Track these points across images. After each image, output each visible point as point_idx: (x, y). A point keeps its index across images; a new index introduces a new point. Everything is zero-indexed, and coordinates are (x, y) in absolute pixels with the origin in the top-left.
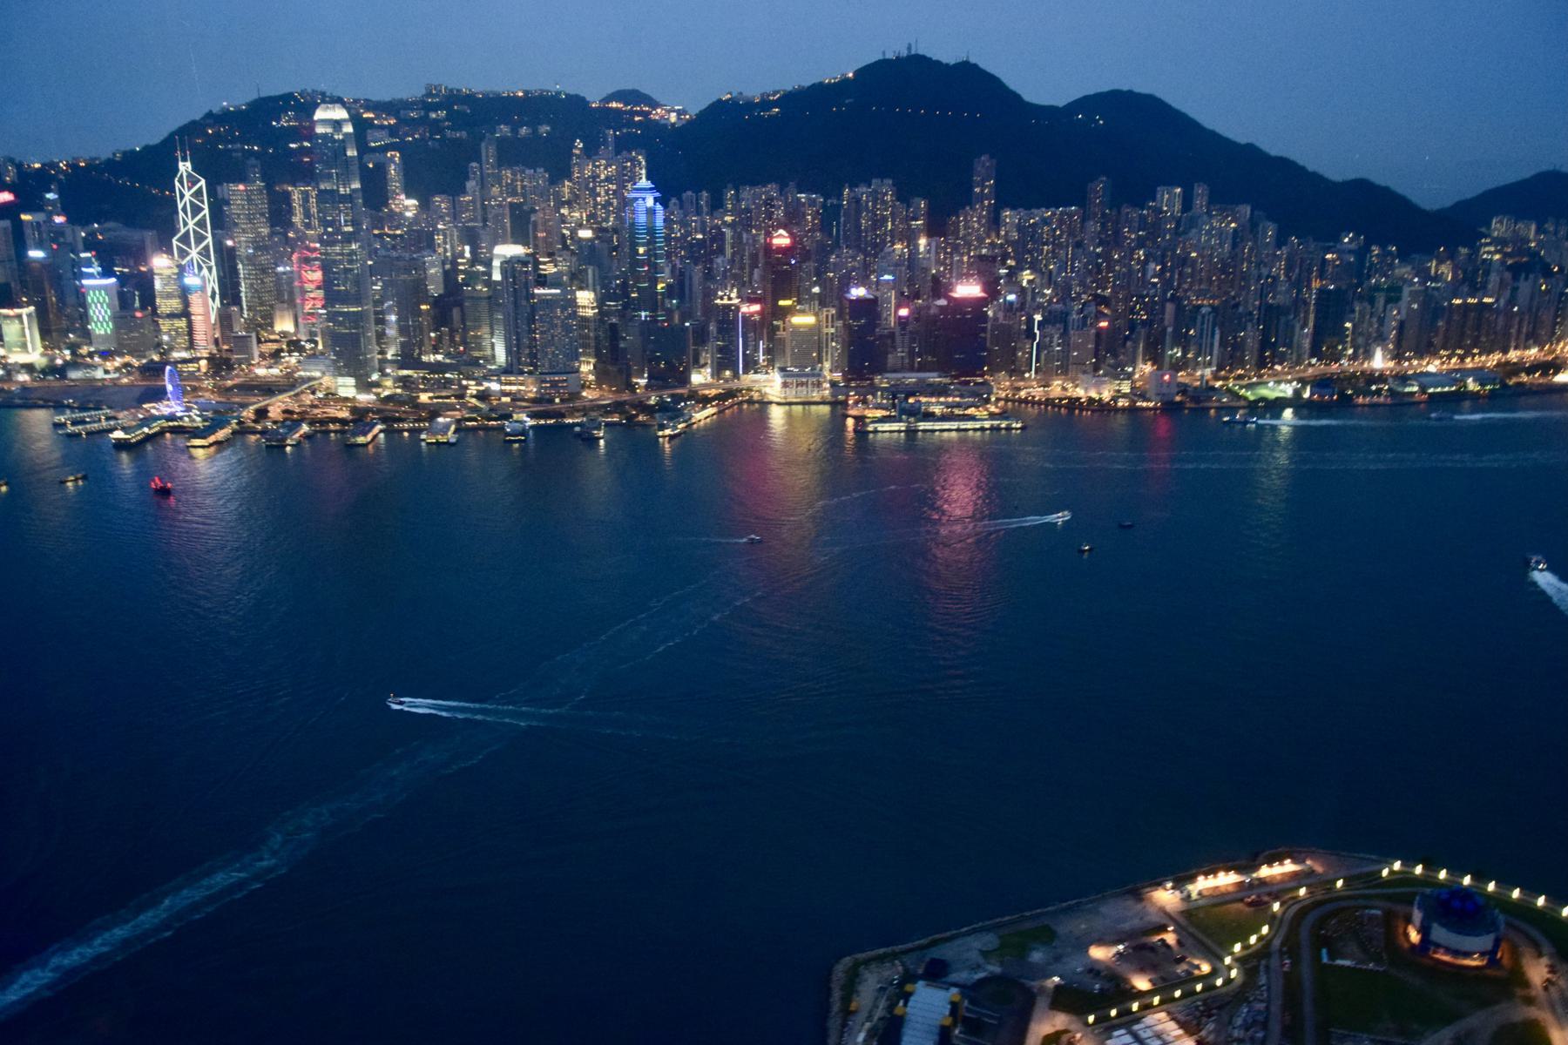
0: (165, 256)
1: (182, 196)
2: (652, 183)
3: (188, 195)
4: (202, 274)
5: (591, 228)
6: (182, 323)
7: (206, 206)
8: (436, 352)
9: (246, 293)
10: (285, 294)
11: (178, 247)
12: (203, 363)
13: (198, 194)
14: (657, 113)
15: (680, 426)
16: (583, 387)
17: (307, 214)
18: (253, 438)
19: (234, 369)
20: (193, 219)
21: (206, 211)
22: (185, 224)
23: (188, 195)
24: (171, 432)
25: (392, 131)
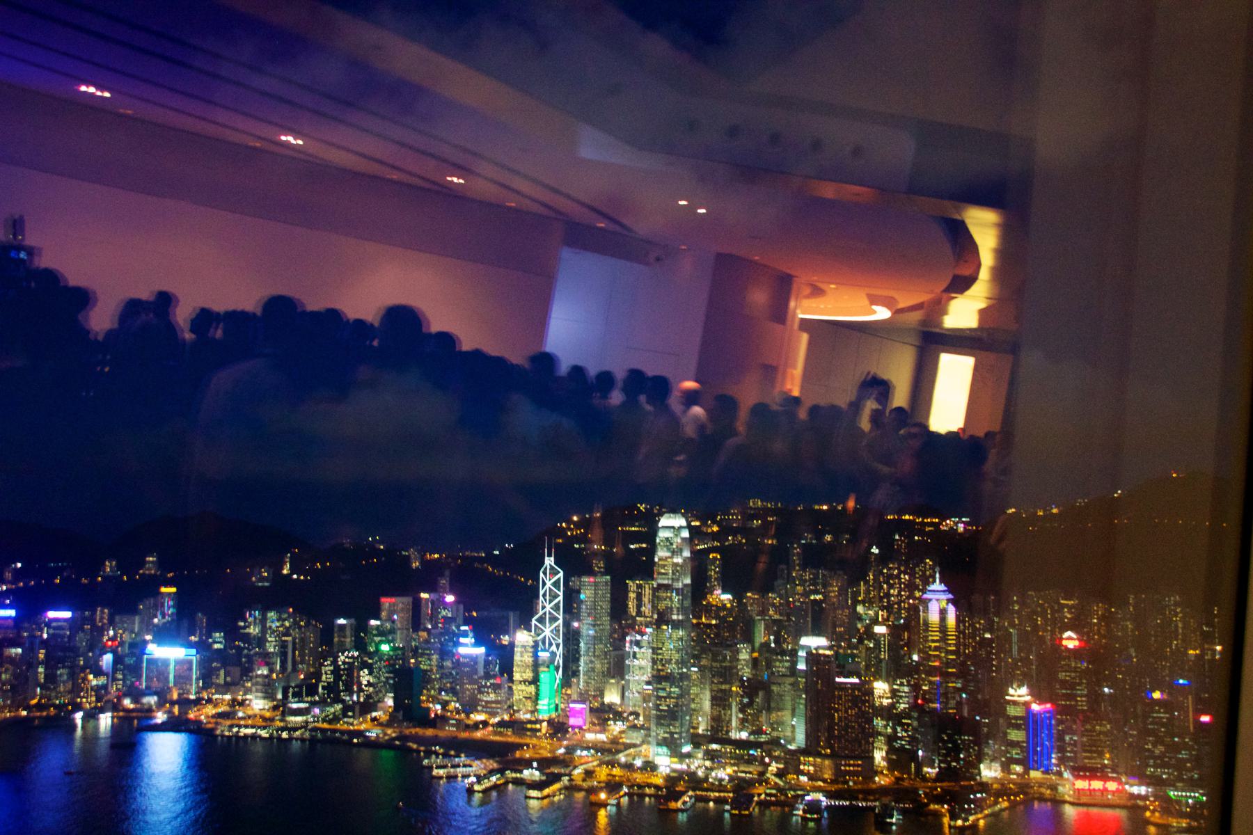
0: (525, 632)
1: (544, 584)
2: (945, 585)
3: (549, 584)
4: (551, 649)
5: (885, 625)
6: (532, 689)
7: (561, 594)
8: (740, 730)
9: (584, 668)
10: (618, 669)
11: (535, 624)
12: (545, 724)
13: (556, 584)
14: (947, 524)
15: (971, 818)
16: (876, 773)
17: (639, 606)
18: (580, 796)
19: (568, 732)
20: (549, 603)
21: (561, 598)
22: (544, 608)
23: (549, 584)
24: (510, 782)
25: (714, 536)
